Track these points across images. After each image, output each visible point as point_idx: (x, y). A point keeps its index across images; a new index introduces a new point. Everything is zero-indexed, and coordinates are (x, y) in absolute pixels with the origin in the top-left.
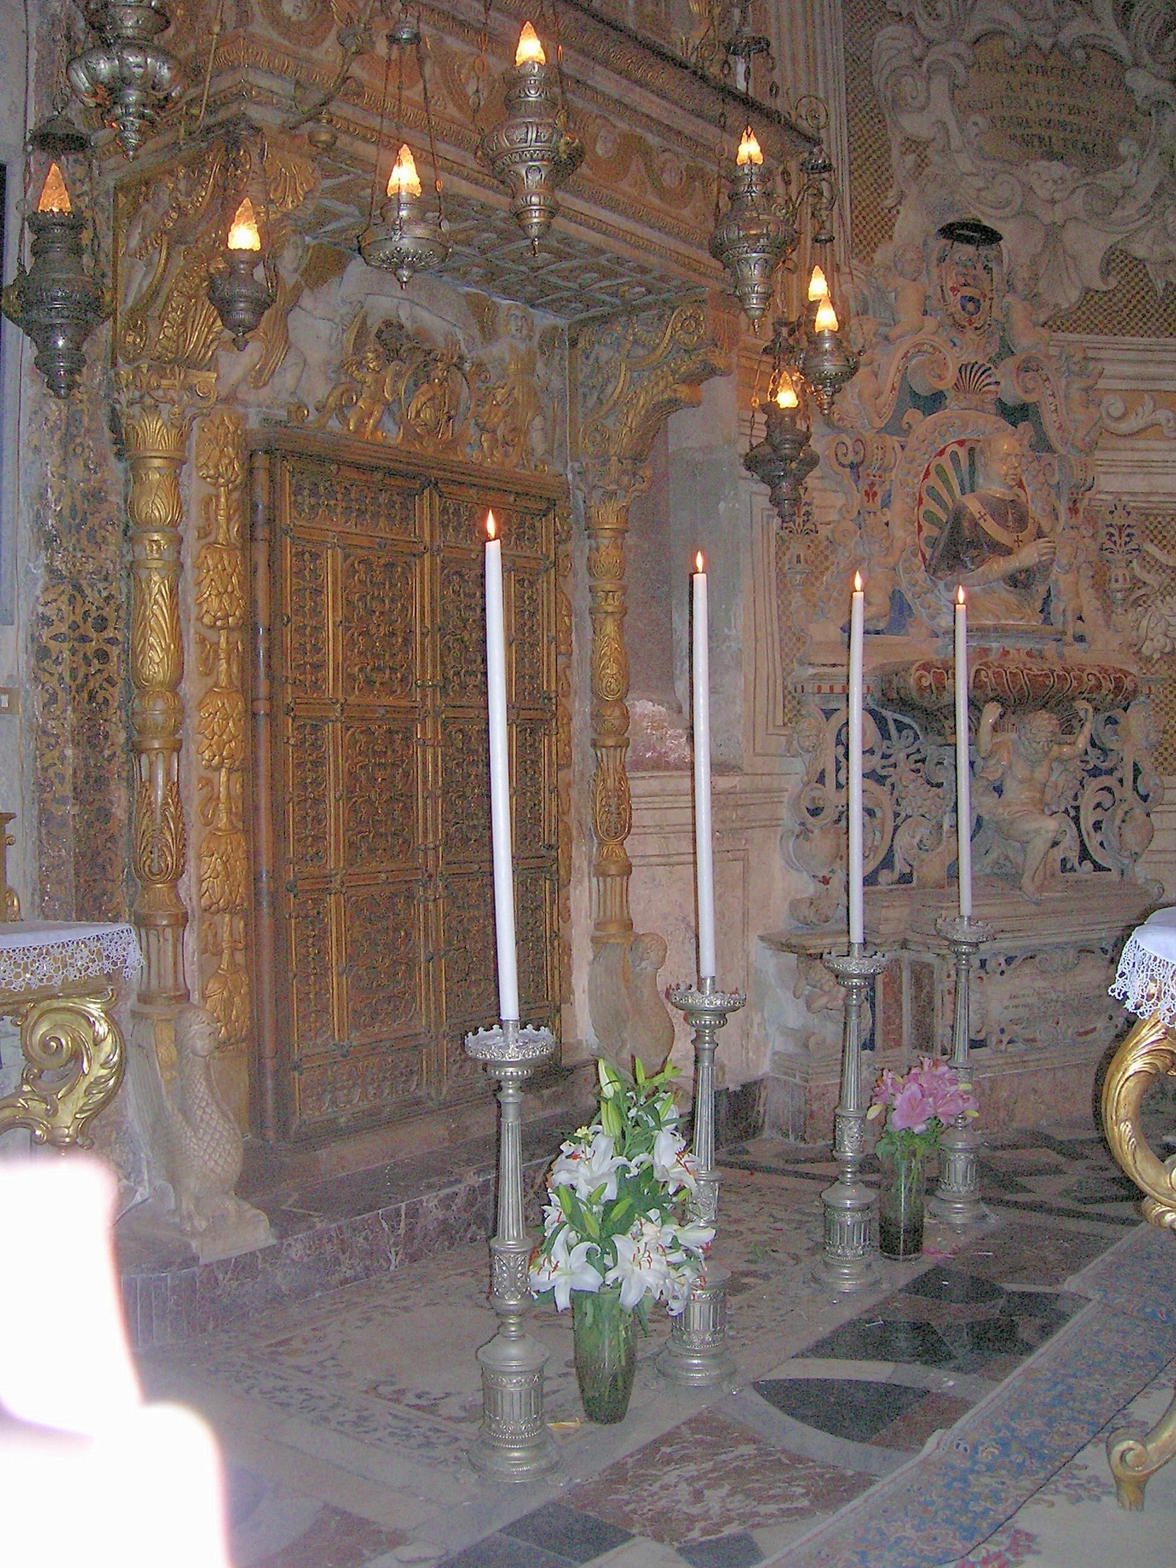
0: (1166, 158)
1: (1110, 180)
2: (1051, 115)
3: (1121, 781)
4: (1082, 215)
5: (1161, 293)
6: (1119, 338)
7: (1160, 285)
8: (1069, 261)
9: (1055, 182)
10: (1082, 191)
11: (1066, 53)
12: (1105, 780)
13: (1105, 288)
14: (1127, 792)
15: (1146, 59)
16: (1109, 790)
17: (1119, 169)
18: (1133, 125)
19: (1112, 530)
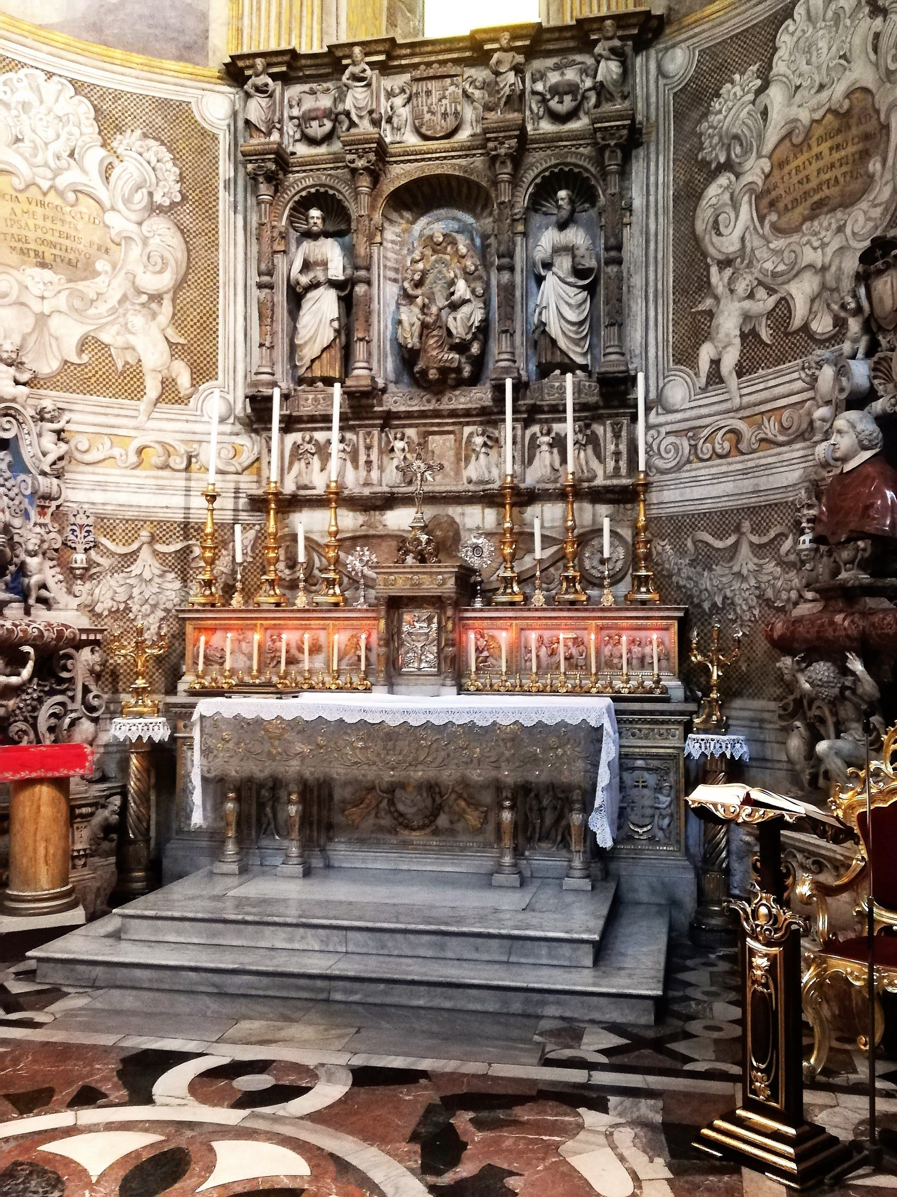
0: (131, 277)
1: (88, 288)
2: (43, 237)
3: (72, 698)
4: (64, 308)
5: (120, 368)
6: (88, 396)
7: (120, 365)
8: (53, 342)
9: (45, 284)
10: (66, 292)
11: (61, 194)
12: (58, 698)
13: (79, 362)
14: (78, 705)
15: (120, 206)
16: (63, 704)
17: (96, 280)
18: (107, 251)
19: (74, 527)
